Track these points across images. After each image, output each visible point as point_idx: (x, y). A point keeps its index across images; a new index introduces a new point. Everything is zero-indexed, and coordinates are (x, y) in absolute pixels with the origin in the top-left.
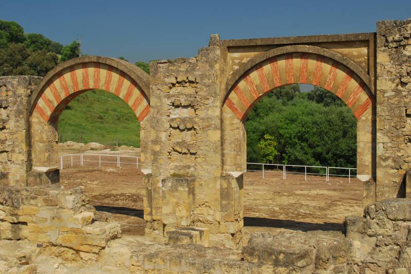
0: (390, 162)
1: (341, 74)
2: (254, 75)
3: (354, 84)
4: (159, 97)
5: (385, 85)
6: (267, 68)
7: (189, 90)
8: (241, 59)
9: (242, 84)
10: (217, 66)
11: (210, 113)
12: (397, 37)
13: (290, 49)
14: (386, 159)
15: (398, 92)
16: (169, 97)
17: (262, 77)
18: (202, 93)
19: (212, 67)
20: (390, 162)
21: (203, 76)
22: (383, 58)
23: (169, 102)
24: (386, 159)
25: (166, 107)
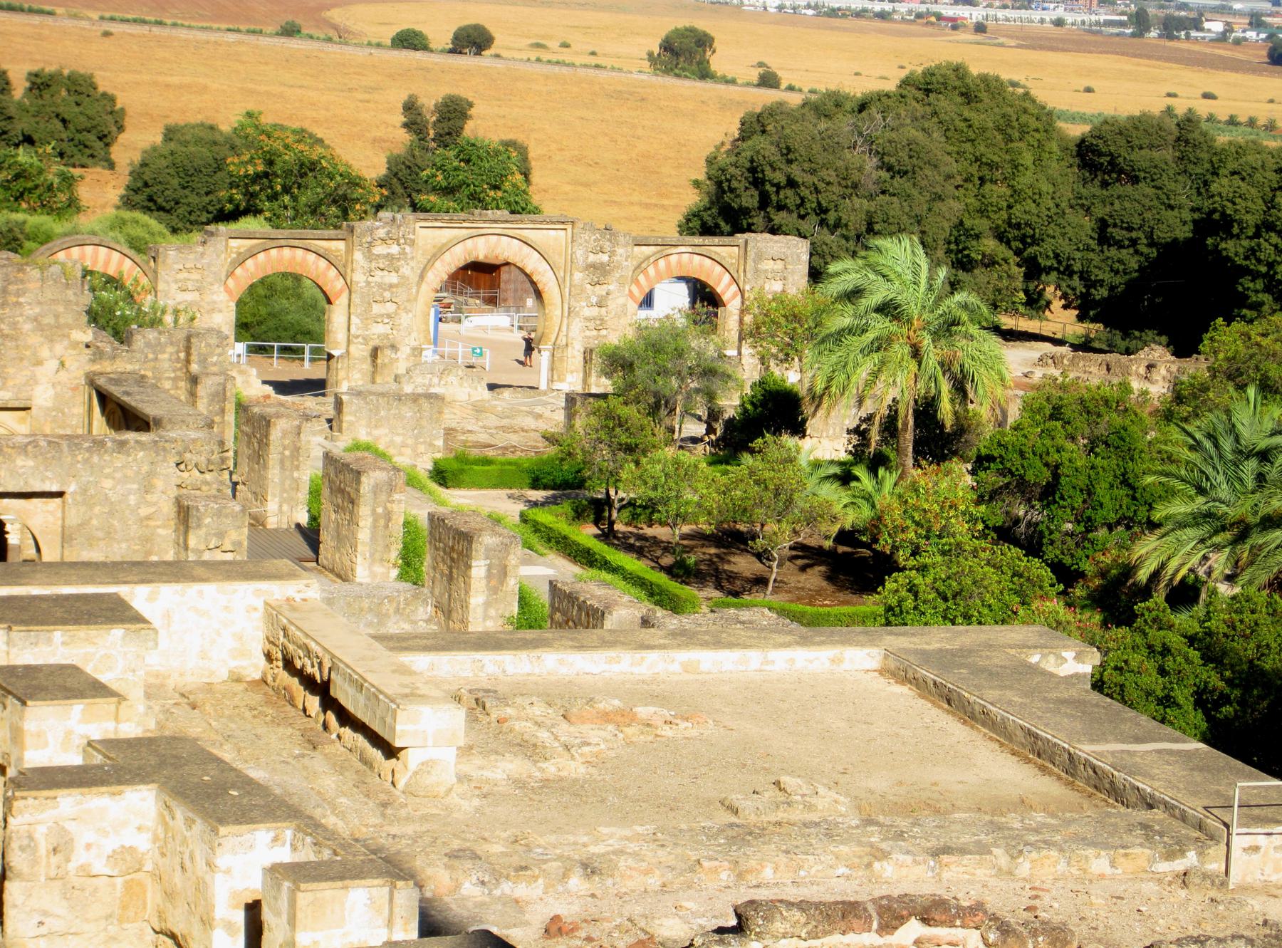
0: (360, 340)
1: (323, 263)
2: (250, 263)
3: (333, 272)
4: (167, 282)
5: (359, 277)
6: (261, 256)
7: (195, 276)
8: (239, 248)
9: (239, 271)
10: (223, 256)
11: (215, 297)
12: (369, 239)
13: (283, 242)
14: (358, 337)
15: (368, 283)
16: (176, 282)
17: (256, 265)
18: (209, 280)
19: (218, 256)
20: (360, 340)
21: (209, 265)
22: (358, 256)
23: (176, 287)
24: (358, 337)
25: (173, 291)
